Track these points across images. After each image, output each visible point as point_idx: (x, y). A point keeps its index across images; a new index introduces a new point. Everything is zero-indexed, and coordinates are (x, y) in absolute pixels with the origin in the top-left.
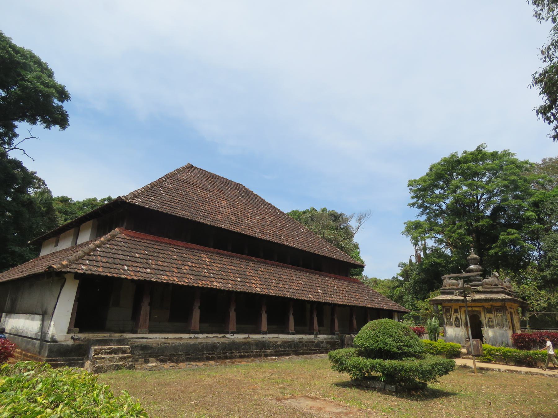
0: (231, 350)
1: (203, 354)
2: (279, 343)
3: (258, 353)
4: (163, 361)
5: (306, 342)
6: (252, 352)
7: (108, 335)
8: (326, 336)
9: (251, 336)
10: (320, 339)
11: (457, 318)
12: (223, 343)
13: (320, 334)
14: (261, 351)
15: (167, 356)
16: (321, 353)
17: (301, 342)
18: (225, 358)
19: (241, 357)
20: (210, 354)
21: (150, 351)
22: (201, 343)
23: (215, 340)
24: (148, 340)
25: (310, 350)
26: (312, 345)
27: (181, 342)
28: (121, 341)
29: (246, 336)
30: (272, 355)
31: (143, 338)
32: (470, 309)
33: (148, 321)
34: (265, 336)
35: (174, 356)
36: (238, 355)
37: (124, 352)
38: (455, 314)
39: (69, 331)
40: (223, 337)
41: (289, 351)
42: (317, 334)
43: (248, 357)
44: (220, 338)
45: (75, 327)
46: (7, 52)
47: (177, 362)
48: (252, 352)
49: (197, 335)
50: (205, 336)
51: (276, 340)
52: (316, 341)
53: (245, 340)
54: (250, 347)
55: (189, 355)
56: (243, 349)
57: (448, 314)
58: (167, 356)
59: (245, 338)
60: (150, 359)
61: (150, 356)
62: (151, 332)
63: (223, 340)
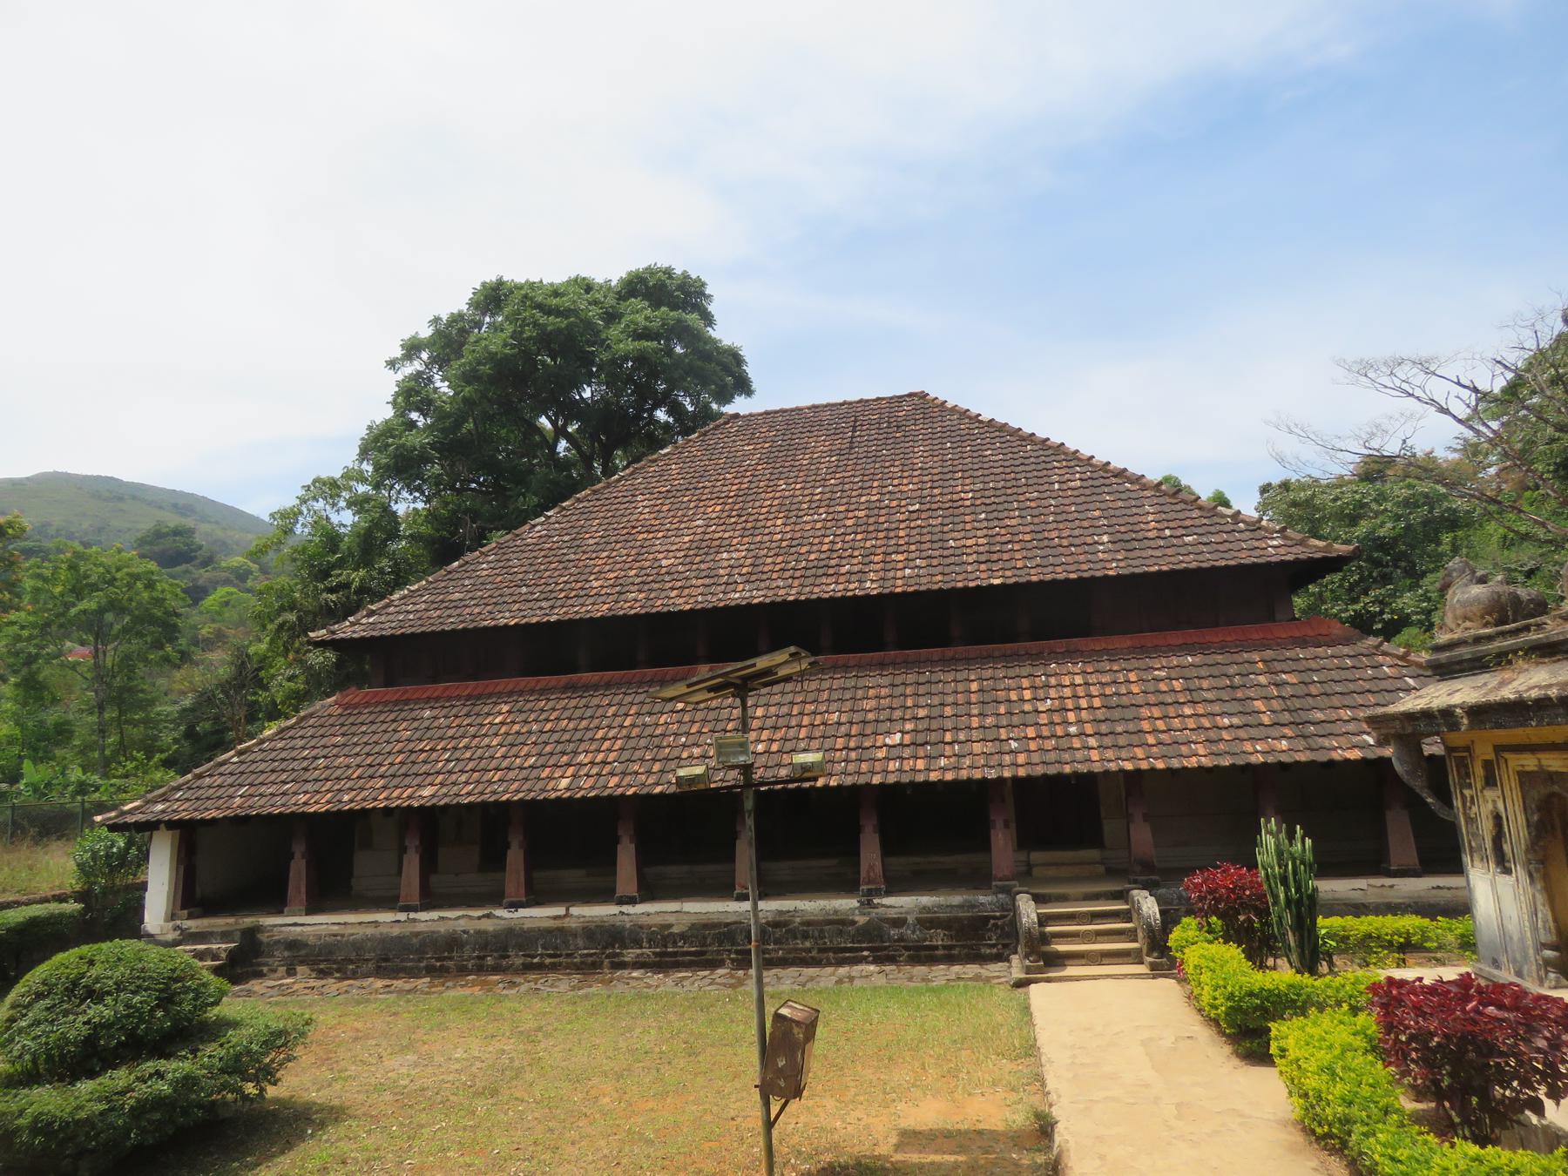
0: (505, 949)
1: (420, 960)
2: (675, 930)
3: (590, 959)
4: (323, 974)
5: (808, 923)
6: (568, 955)
7: (231, 920)
8: (926, 900)
9: (575, 911)
10: (892, 914)
11: (1497, 818)
12: (478, 932)
13: (889, 893)
14: (602, 953)
15: (335, 962)
16: (877, 961)
17: (776, 925)
18: (480, 969)
19: (528, 968)
20: (438, 960)
21: (303, 952)
22: (417, 934)
23: (463, 924)
24: (305, 929)
25: (821, 951)
26: (840, 933)
27: (370, 931)
28: (225, 936)
29: (560, 911)
30: (637, 965)
31: (295, 924)
32: (1529, 762)
33: (303, 890)
34: (625, 909)
35: (351, 962)
36: (519, 961)
37: (215, 957)
38: (1489, 794)
39: (172, 916)
40: (488, 916)
41: (718, 952)
42: (870, 893)
43: (554, 968)
44: (479, 918)
45: (183, 908)
46: (536, 324)
47: (354, 976)
48: (568, 955)
49: (412, 915)
50: (434, 915)
51: (671, 919)
52: (861, 920)
53: (558, 923)
54: (566, 943)
55: (386, 960)
56: (544, 948)
57: (1467, 792)
58: (335, 962)
59: (555, 918)
60: (299, 968)
61: (302, 963)
62: (310, 911)
63: (488, 926)
